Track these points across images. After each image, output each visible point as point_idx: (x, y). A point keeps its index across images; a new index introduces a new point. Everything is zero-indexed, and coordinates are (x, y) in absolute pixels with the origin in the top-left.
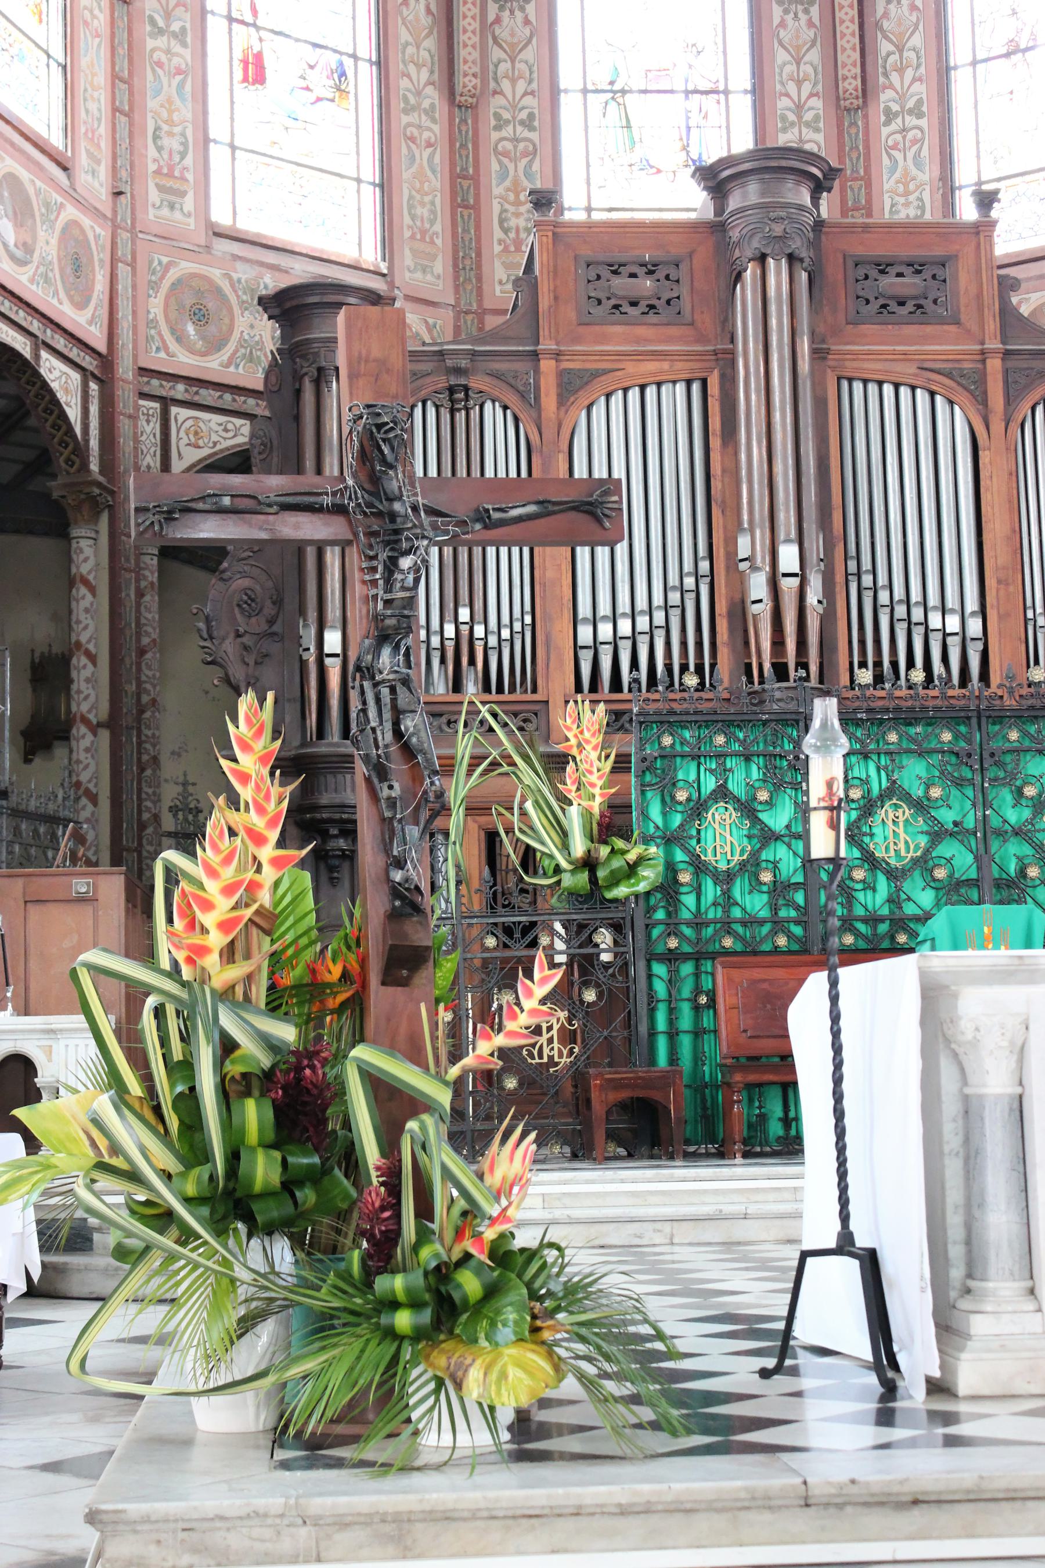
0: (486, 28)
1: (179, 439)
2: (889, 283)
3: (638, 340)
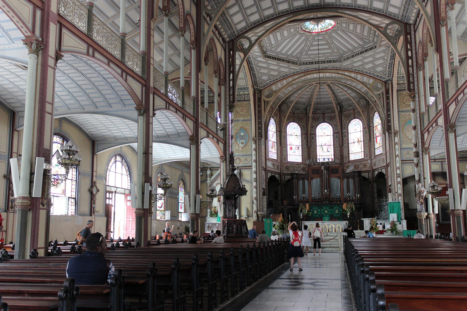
0: (311, 141)
2: (334, 171)
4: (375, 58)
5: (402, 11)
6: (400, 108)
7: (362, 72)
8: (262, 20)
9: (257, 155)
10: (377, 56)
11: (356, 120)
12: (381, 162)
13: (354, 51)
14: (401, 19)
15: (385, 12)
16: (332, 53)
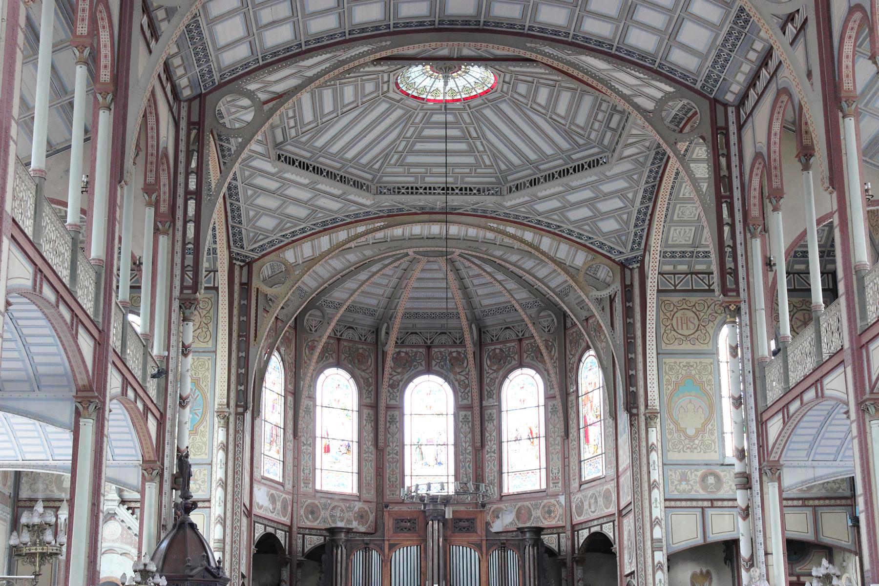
1: (307, 543)
2: (462, 524)
3: (406, 537)
4: (600, 191)
5: (709, 63)
6: (663, 345)
7: (556, 231)
8: (300, 45)
9: (230, 464)
10: (607, 188)
11: (526, 371)
12: (601, 501)
13: (542, 167)
14: (703, 87)
15: (658, 61)
16: (477, 165)
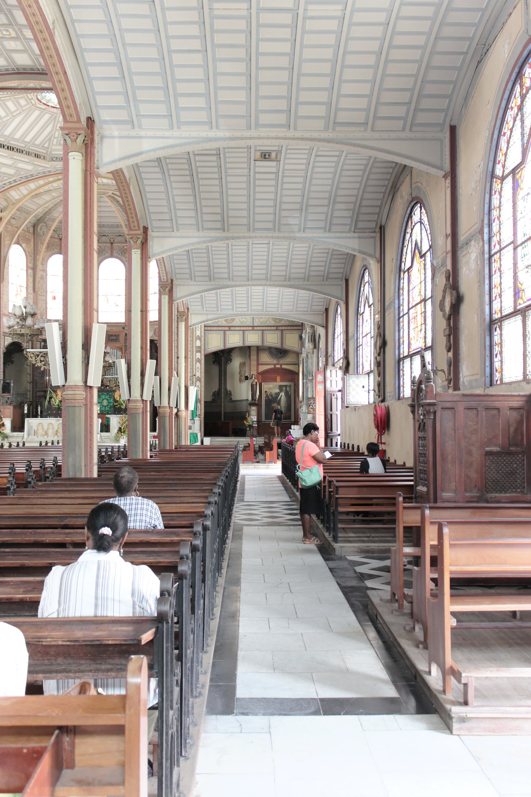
2: (112, 338)
